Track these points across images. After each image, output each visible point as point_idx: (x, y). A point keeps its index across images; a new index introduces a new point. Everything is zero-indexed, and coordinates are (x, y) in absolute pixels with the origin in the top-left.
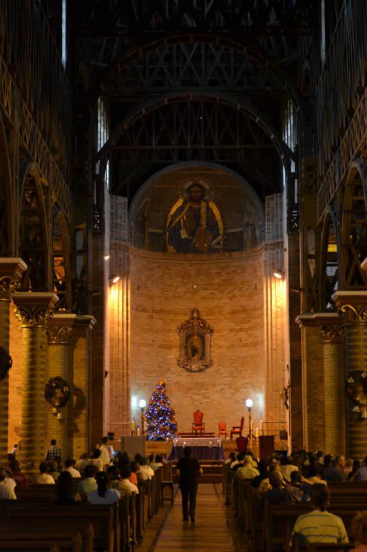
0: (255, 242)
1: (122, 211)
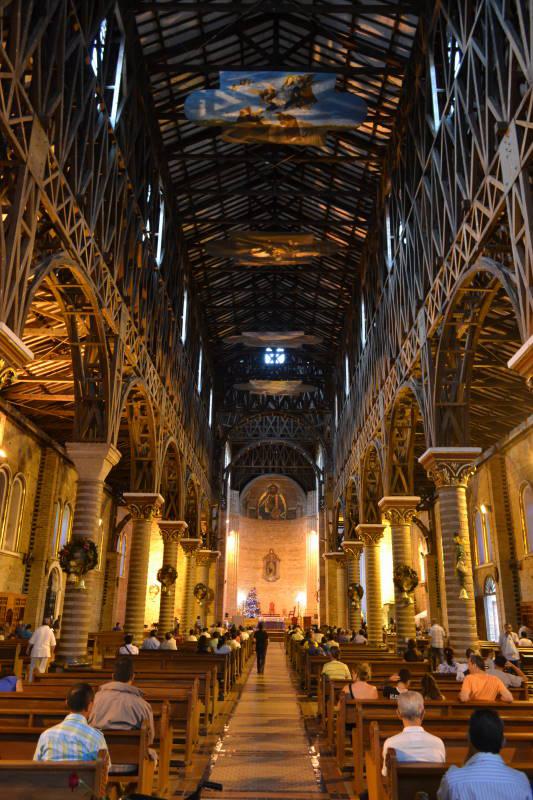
0: (302, 515)
1: (236, 498)
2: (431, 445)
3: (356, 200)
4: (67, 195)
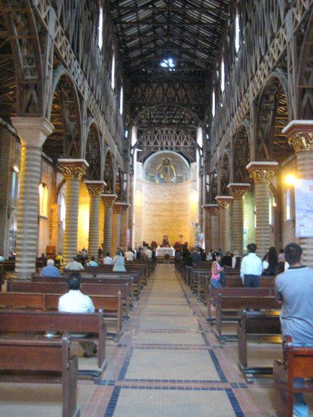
1: (140, 168)
2: (293, 119)
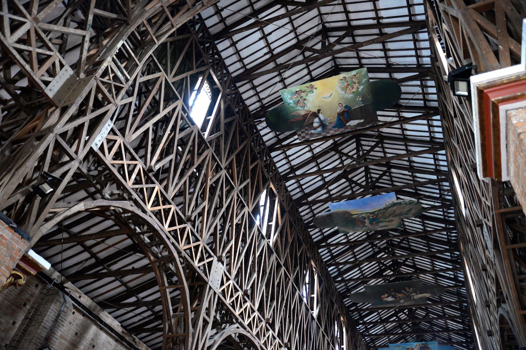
3: (449, 254)
4: (237, 291)
